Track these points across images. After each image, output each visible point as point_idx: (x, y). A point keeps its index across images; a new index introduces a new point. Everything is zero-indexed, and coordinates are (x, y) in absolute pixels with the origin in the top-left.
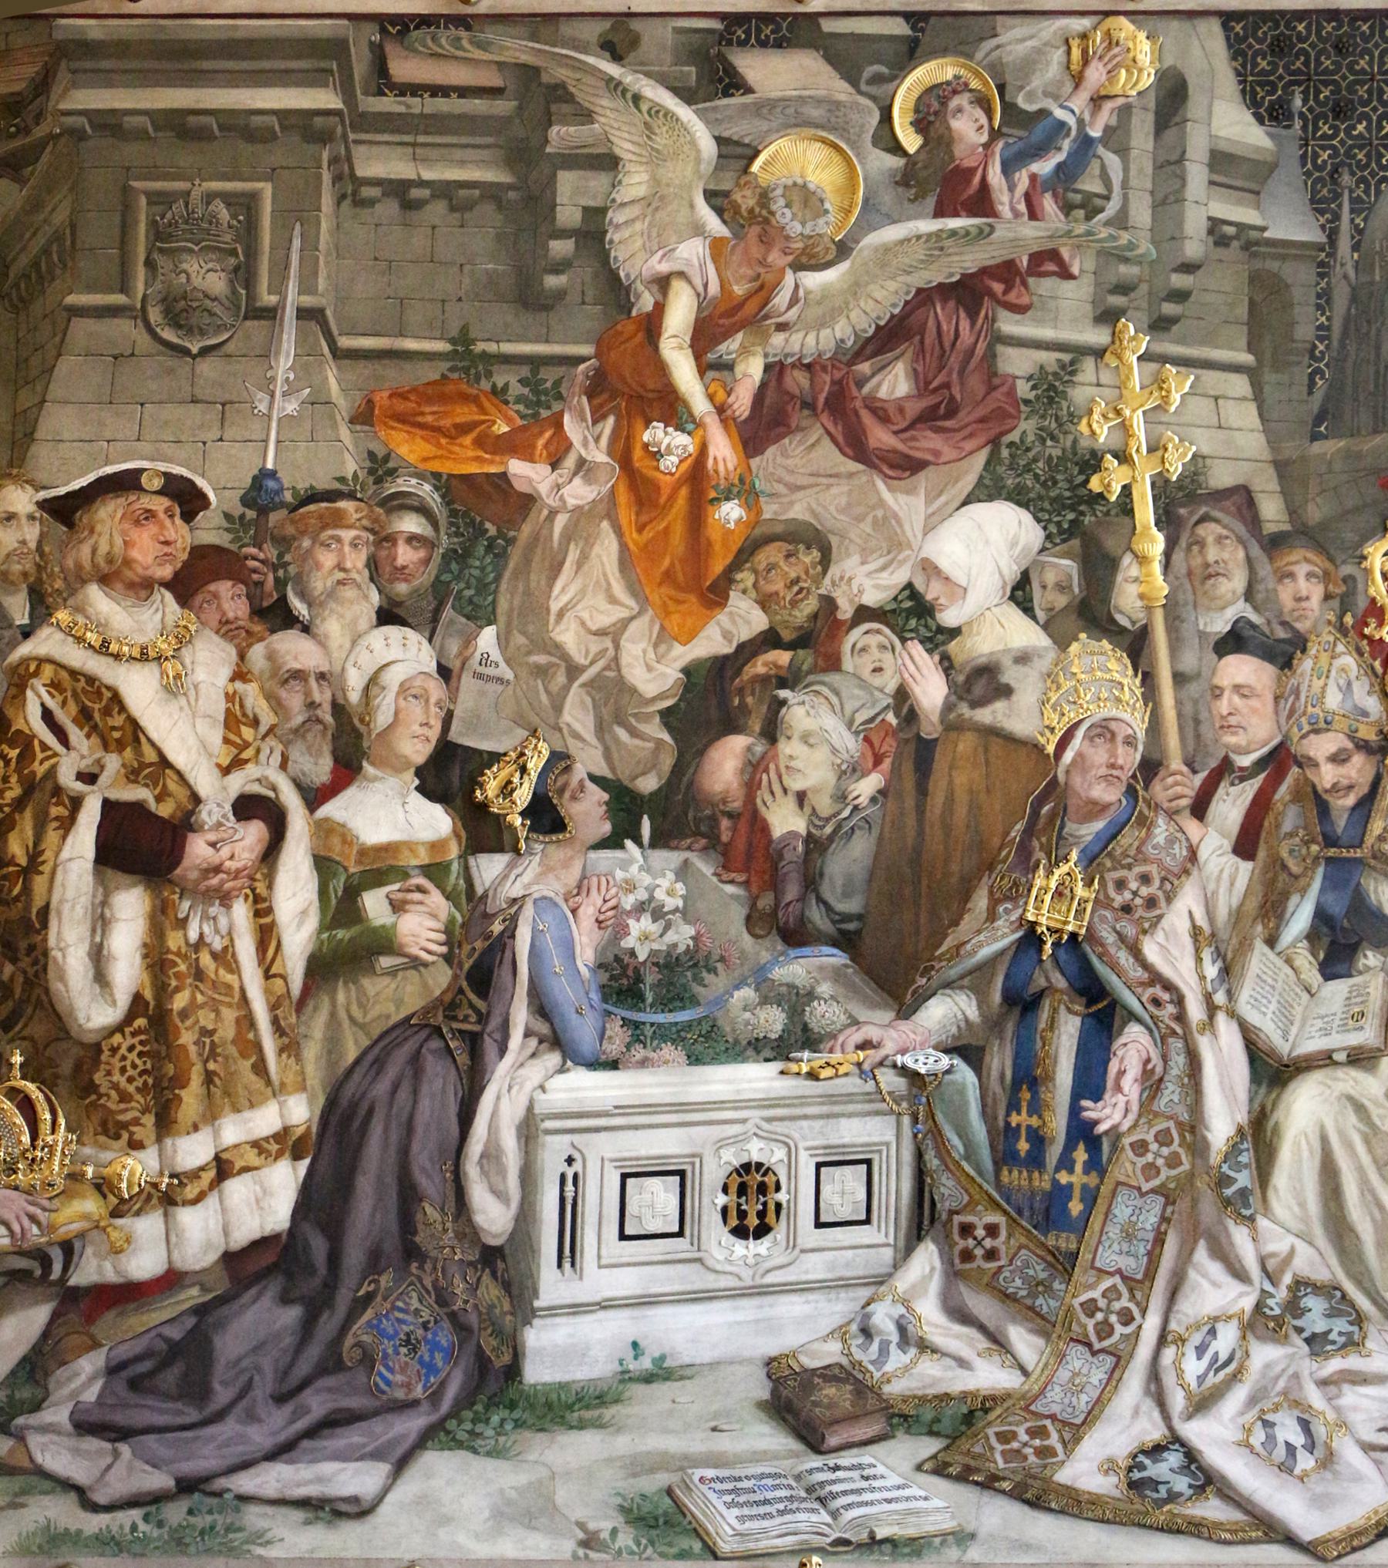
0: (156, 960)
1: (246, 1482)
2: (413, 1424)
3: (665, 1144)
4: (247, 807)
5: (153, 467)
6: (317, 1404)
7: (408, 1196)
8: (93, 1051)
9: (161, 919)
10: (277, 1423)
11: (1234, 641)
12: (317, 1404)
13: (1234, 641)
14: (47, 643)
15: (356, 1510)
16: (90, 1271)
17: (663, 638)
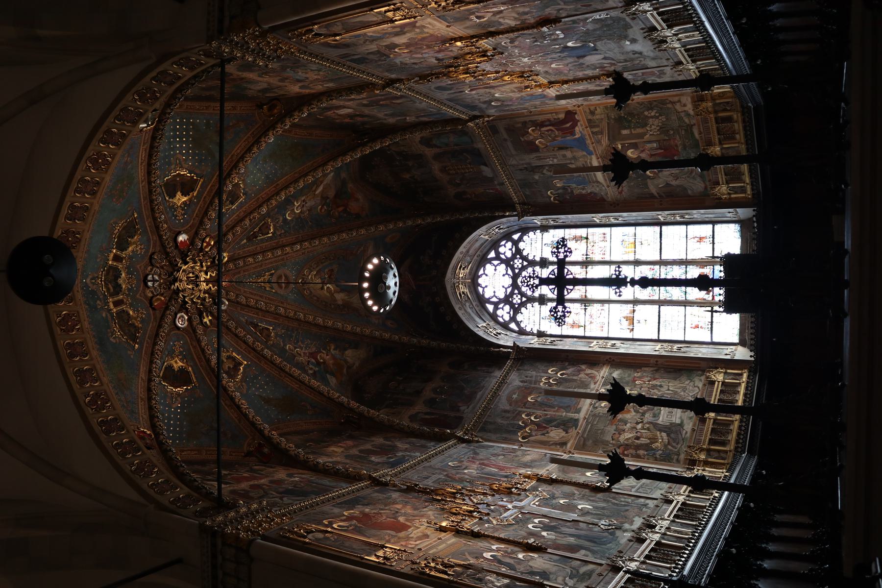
0: (646, 438)
1: (683, 436)
2: (681, 429)
3: (665, 416)
4: (636, 433)
5: (611, 435)
6: (679, 433)
7: (666, 428)
8: (651, 442)
9: (643, 438)
10: (680, 435)
11: (641, 389)
12: (679, 433)
13: (641, 389)
14: (622, 442)
15: (686, 433)
16: (667, 443)
17: (632, 412)
